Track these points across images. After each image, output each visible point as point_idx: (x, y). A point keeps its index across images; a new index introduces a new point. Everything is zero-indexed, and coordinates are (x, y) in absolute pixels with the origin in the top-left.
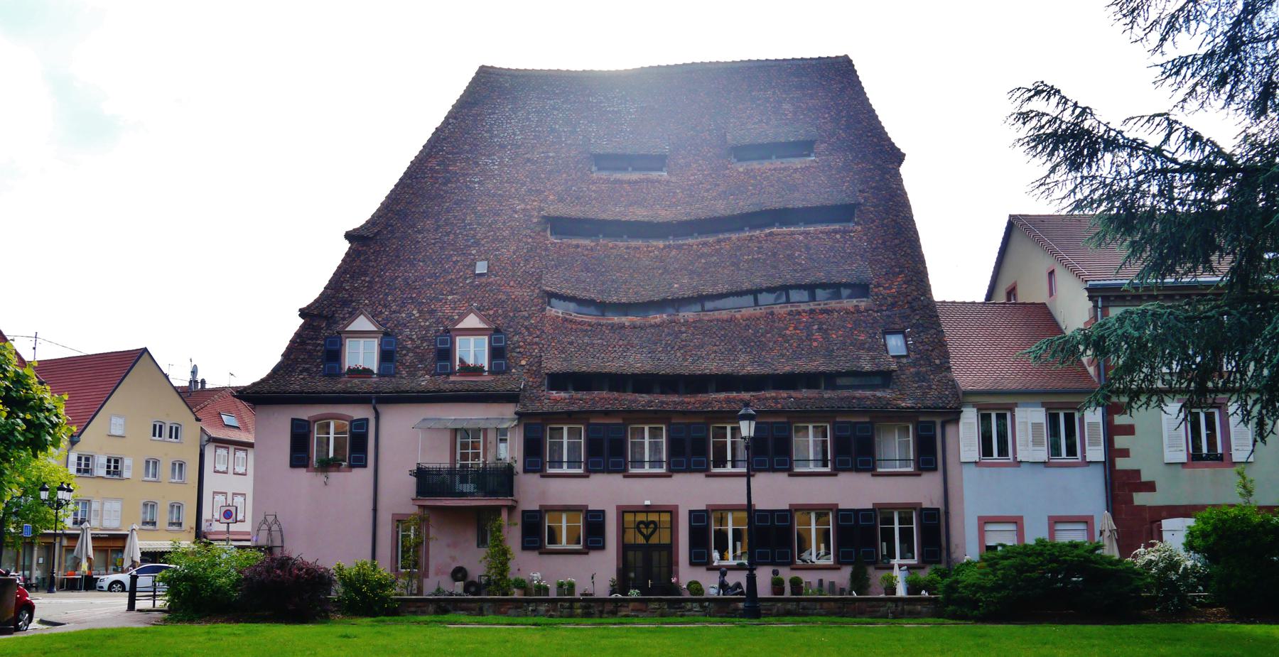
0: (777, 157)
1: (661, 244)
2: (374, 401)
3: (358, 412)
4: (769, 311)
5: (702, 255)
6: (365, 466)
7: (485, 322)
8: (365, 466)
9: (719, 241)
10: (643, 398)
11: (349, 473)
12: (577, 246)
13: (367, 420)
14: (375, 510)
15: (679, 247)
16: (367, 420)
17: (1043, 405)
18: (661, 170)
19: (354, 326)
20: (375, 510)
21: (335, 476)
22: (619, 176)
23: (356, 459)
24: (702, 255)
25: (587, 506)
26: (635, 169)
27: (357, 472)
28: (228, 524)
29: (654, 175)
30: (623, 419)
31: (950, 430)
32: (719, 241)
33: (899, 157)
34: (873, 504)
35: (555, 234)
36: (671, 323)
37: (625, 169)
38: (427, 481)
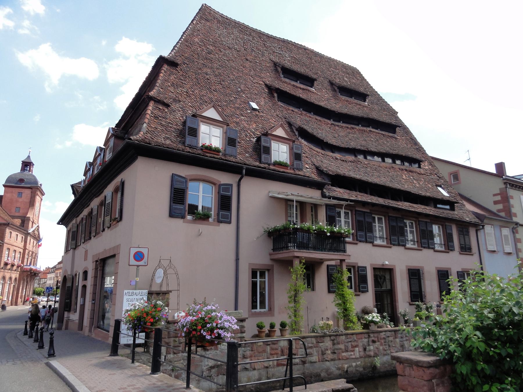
2: (244, 171)
4: (391, 166)
6: (230, 223)
7: (287, 135)
8: (230, 223)
10: (381, 201)
11: (217, 227)
13: (231, 185)
14: (237, 259)
15: (338, 126)
16: (231, 185)
18: (312, 88)
19: (206, 114)
20: (237, 259)
21: (202, 227)
23: (223, 216)
25: (357, 263)
27: (223, 227)
28: (138, 266)
30: (370, 210)
31: (481, 234)
32: (353, 128)
34: (462, 269)
35: (281, 101)
36: (359, 162)
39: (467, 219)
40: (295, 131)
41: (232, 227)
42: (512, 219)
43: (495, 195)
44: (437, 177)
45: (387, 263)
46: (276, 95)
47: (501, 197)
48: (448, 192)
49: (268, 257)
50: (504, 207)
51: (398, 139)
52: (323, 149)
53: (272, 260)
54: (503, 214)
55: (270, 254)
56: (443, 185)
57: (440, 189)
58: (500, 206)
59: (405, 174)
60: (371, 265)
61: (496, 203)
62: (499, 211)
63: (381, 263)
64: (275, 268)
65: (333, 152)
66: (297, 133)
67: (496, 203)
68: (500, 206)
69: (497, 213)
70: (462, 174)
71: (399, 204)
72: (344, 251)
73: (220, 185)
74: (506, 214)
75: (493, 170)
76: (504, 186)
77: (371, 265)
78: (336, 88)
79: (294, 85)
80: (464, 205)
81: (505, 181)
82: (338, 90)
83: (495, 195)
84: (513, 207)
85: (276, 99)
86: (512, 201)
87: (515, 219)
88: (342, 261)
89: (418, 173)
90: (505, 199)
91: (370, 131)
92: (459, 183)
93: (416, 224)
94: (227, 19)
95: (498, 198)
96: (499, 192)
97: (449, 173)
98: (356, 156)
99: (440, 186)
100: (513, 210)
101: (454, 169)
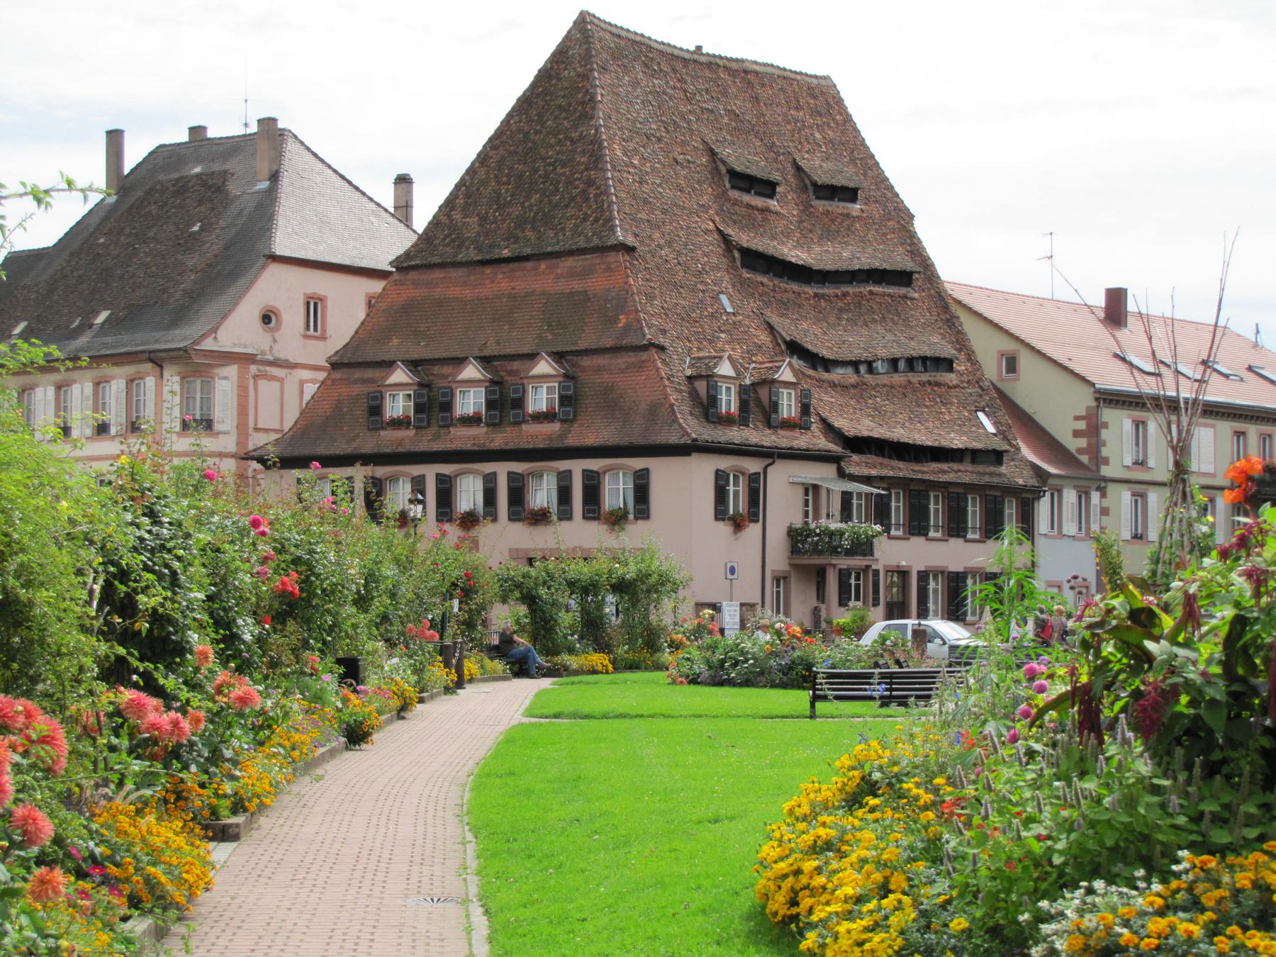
0: (840, 200)
1: (810, 290)
3: (753, 466)
5: (841, 310)
6: (757, 521)
9: (845, 295)
12: (762, 284)
13: (759, 474)
17: (1075, 487)
22: (746, 198)
24: (841, 310)
26: (758, 194)
29: (773, 204)
32: (845, 295)
33: (912, 217)
37: (748, 191)
38: (796, 537)
39: (1021, 482)
40: (780, 341)
41: (760, 524)
42: (1098, 470)
43: (1077, 418)
44: (979, 390)
45: (904, 563)
46: (737, 254)
47: (1088, 425)
48: (996, 424)
49: (787, 561)
50: (1089, 444)
51: (914, 299)
52: (814, 368)
53: (791, 565)
54: (1084, 459)
55: (789, 558)
56: (988, 406)
57: (981, 415)
58: (1082, 443)
59: (929, 394)
60: (884, 566)
61: (1077, 434)
62: (1080, 451)
63: (895, 563)
64: (793, 574)
65: (827, 370)
66: (783, 347)
67: (1077, 434)
68: (1082, 443)
69: (1077, 455)
70: (1025, 360)
71: (925, 469)
72: (872, 555)
73: (750, 475)
74: (1090, 459)
75: (1100, 301)
76: (1093, 404)
77: (884, 566)
78: (808, 182)
79: (748, 206)
80: (1018, 449)
81: (1098, 395)
82: (810, 188)
83: (1077, 418)
84: (1104, 445)
85: (738, 263)
86: (1105, 434)
87: (1106, 471)
88: (868, 567)
89: (950, 387)
90: (1093, 429)
91: (871, 292)
92: (1017, 379)
93: (943, 497)
94: (619, 36)
95: (1082, 425)
96: (1083, 413)
97: (998, 352)
98: (857, 371)
99: (983, 411)
100: (1105, 452)
101: (1010, 346)
